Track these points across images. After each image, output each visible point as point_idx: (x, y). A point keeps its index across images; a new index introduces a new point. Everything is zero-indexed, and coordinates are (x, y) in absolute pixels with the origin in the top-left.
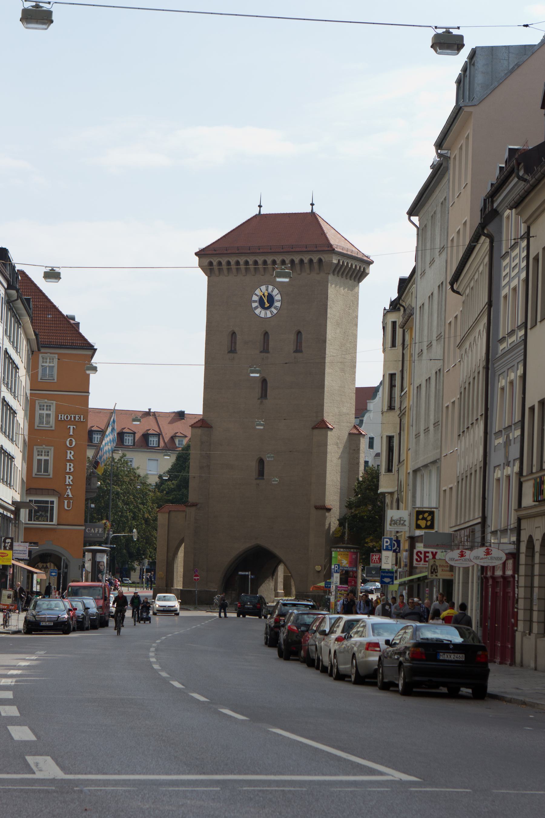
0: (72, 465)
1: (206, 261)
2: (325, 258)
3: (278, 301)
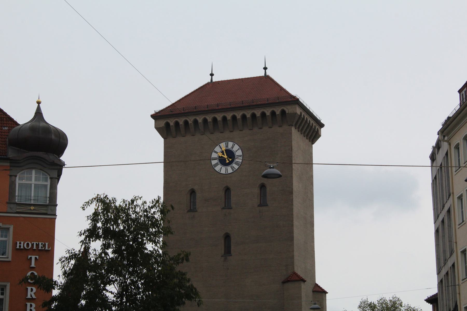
0: (34, 305)
1: (162, 123)
2: (289, 109)
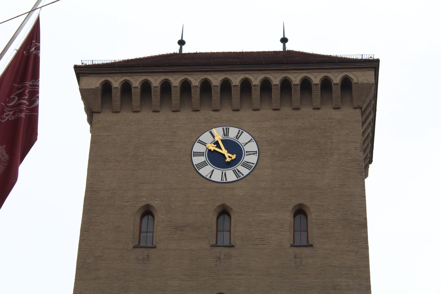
3: (250, 153)
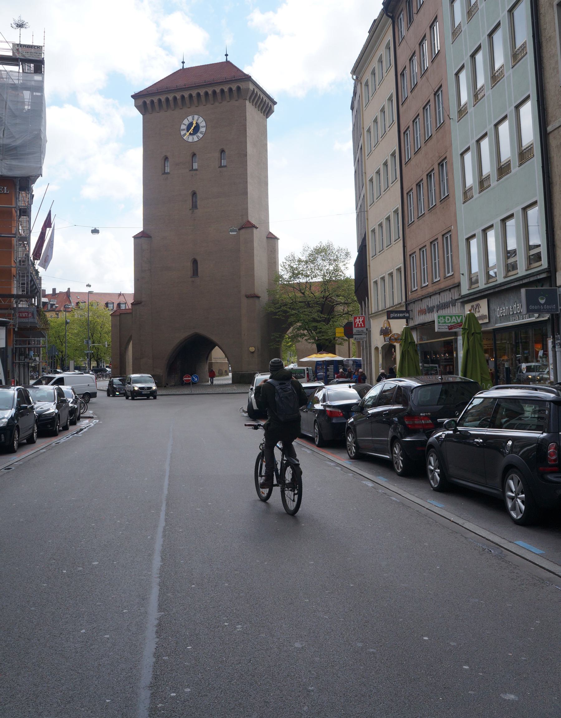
1: (141, 102)
2: (243, 85)
3: (203, 127)
